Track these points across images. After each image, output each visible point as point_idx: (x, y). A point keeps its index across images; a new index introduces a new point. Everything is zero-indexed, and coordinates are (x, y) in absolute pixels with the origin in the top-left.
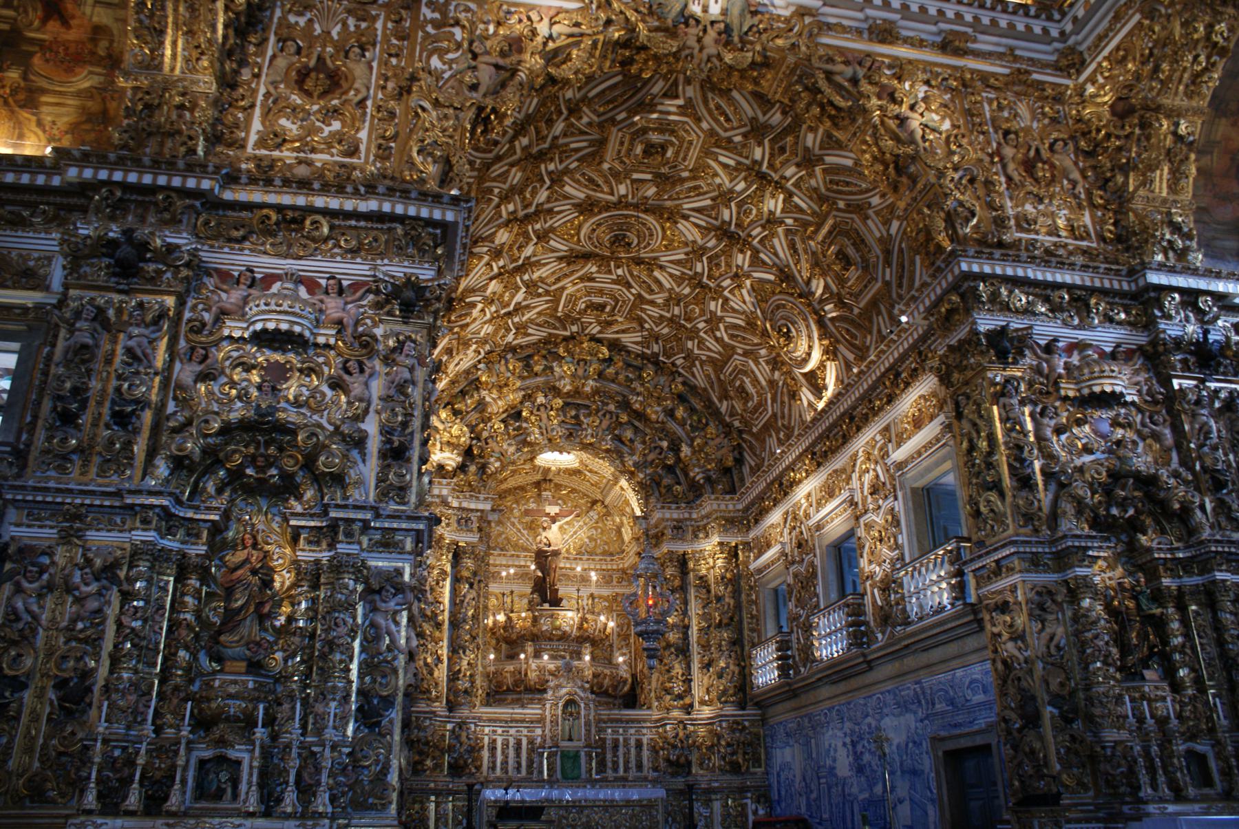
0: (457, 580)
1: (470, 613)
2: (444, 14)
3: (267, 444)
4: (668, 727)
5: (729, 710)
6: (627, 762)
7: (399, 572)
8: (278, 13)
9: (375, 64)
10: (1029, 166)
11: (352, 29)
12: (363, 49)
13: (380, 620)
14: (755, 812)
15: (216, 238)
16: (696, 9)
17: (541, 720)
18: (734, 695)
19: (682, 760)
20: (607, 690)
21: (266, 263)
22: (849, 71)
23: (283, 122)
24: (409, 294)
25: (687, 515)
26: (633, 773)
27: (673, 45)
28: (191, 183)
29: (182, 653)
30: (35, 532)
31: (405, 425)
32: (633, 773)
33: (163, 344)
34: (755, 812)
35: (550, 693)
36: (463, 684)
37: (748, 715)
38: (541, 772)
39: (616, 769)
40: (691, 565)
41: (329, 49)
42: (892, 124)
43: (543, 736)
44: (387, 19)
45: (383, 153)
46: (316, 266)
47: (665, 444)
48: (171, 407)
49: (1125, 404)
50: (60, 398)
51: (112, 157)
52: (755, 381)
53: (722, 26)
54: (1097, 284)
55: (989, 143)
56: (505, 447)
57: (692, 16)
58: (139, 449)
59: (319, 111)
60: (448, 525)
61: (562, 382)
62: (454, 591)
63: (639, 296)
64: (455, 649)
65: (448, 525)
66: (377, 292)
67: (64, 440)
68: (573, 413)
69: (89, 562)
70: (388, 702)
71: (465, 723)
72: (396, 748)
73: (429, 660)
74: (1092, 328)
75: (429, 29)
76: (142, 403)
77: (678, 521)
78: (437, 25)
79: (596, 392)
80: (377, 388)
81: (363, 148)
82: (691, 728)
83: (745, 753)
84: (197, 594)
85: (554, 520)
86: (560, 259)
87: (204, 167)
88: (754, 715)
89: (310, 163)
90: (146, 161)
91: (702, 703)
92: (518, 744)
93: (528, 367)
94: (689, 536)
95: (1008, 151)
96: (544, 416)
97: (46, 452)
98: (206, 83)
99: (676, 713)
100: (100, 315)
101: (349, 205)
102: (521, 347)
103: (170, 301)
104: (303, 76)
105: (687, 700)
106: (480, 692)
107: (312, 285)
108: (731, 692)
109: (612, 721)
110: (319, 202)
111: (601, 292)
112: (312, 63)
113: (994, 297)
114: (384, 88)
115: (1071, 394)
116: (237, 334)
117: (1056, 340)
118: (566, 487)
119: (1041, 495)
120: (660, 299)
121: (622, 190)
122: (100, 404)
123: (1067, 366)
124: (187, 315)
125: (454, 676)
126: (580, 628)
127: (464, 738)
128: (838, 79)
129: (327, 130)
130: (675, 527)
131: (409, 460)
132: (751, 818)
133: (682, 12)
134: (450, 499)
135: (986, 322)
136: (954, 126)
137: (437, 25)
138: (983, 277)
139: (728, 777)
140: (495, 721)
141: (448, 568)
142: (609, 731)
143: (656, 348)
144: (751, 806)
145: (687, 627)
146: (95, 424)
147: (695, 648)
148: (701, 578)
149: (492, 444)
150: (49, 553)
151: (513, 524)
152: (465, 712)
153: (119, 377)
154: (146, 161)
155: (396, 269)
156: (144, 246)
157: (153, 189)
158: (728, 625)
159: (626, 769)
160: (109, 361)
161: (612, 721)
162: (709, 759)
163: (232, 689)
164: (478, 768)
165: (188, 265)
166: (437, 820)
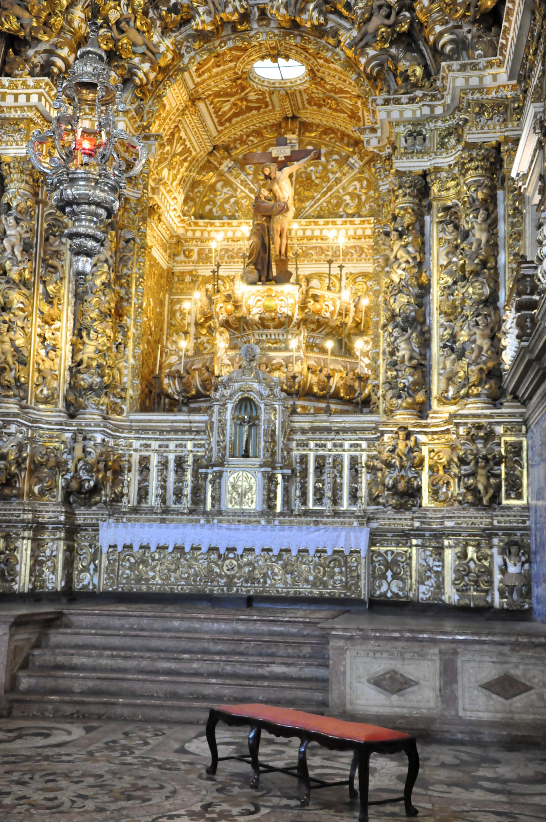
1: (98, 282)
4: (386, 437)
14: (504, 570)
18: (480, 383)
19: (402, 486)
20: (337, 392)
25: (426, 111)
26: (345, 505)
34: (504, 570)
35: (221, 389)
37: (500, 415)
38: (204, 502)
40: (435, 189)
71: (80, 431)
73: (20, 342)
77: (417, 123)
82: (422, 438)
83: (491, 475)
85: (282, 165)
88: (511, 415)
91: (444, 400)
92: (180, 463)
94: (433, 141)
105: (420, 397)
106: (130, 392)
108: (473, 378)
118: (318, 126)
126: (303, 306)
127: (78, 452)
130: (410, 134)
132: (497, 576)
139: (472, 512)
140: (145, 430)
142: (312, 444)
144: (498, 560)
148: (446, 209)
158: (476, 274)
161: (314, 430)
162: (448, 483)
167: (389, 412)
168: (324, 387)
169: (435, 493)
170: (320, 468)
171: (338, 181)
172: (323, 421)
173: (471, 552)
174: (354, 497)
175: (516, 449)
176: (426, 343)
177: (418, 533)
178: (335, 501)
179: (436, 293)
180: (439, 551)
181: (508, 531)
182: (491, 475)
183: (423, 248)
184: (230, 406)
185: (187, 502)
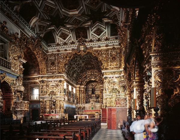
10: (113, 58)
46: (55, 79)
58: (46, 94)
78: (61, 56)
95: (111, 57)
100: (42, 86)
113: (106, 74)
123: (112, 79)
137: (61, 56)
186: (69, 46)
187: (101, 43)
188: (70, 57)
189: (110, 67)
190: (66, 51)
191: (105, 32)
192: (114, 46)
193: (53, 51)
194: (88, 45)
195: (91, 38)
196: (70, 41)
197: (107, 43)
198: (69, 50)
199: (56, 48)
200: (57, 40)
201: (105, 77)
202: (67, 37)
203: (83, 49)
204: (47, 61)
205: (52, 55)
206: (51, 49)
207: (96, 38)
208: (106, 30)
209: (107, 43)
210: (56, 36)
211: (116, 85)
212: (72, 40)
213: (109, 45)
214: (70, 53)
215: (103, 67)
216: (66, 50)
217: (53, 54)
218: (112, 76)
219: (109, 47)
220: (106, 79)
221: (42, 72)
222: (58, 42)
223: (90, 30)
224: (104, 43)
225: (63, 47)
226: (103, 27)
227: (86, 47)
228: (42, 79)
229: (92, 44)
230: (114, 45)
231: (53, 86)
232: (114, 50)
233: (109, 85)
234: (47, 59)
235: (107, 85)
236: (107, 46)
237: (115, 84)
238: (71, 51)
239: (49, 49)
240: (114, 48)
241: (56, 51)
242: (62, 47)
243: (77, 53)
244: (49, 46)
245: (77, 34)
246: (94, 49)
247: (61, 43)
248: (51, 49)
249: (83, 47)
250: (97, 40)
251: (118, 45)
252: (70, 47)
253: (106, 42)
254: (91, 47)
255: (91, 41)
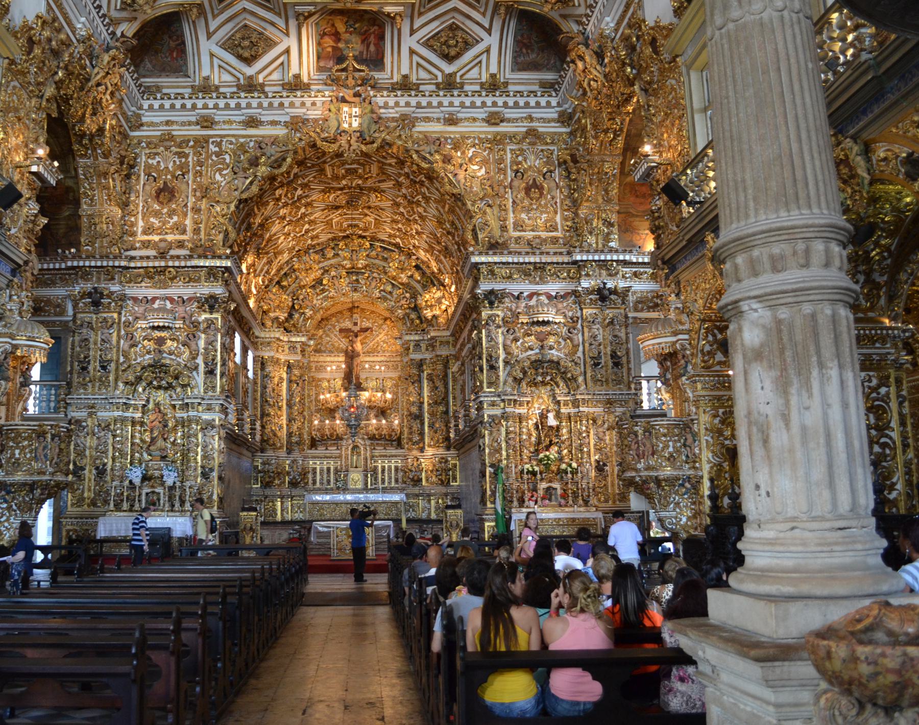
0: (290, 381)
2: (220, 148)
3: (160, 372)
5: (441, 451)
6: (390, 478)
7: (214, 420)
8: (144, 159)
9: (190, 182)
10: (528, 190)
11: (178, 163)
12: (183, 175)
13: (208, 441)
15: (130, 282)
16: (346, 126)
17: (340, 457)
19: (416, 478)
21: (152, 292)
22: (428, 149)
23: (152, 220)
24: (212, 301)
27: (334, 147)
28: (117, 264)
29: (137, 454)
30: (79, 414)
31: (213, 360)
32: (393, 484)
33: (115, 334)
36: (294, 439)
39: (383, 482)
40: (425, 367)
41: (169, 177)
42: (450, 175)
43: (341, 465)
44: (194, 154)
45: (197, 231)
47: (408, 295)
48: (122, 359)
49: (556, 323)
50: (80, 362)
51: (84, 256)
52: (444, 266)
53: (358, 134)
54: (549, 261)
55: (506, 178)
56: (315, 302)
57: (344, 131)
58: (111, 378)
59: (167, 213)
60: (283, 351)
61: (345, 262)
62: (289, 389)
63: (376, 219)
64: (290, 420)
65: (283, 351)
66: (198, 302)
67: (84, 379)
68: (354, 278)
69: (99, 425)
70: (212, 470)
72: (216, 486)
74: (545, 283)
75: (214, 158)
76: (110, 361)
78: (218, 154)
79: (365, 267)
80: (202, 344)
81: (188, 229)
83: (447, 475)
84: (140, 432)
85: (356, 336)
86: (323, 210)
87: (121, 257)
89: (165, 240)
90: (98, 256)
91: (430, 446)
93: (323, 255)
94: (423, 349)
95: (516, 183)
96: (336, 283)
97: (79, 383)
98: (118, 212)
99: (415, 453)
101: (183, 264)
102: (318, 244)
103: (115, 315)
104: (159, 192)
105: (421, 445)
107: (172, 300)
109: (381, 456)
110: (170, 264)
111: (353, 219)
112: (162, 186)
113: (492, 272)
114: (195, 196)
115: (525, 321)
116: (144, 326)
117: (522, 293)
119: (501, 373)
120: (388, 220)
121: (344, 182)
122: (95, 362)
123: (527, 307)
124: (123, 319)
125: (290, 435)
127: (295, 468)
128: (423, 153)
129: (172, 221)
131: (216, 375)
133: (338, 128)
134: (281, 338)
135: (485, 286)
136: (487, 173)
137: (218, 154)
138: (482, 263)
139: (440, 487)
140: (315, 457)
141: (285, 376)
143: (398, 240)
145: (423, 403)
146: (94, 370)
147: (426, 415)
149: (307, 302)
150: (85, 421)
151: (336, 336)
152: (296, 454)
153: (101, 350)
154: (98, 256)
155: (205, 289)
156: (102, 294)
157: (102, 267)
159: (390, 483)
160: (95, 344)
161: (381, 456)
163: (156, 467)
164: (307, 483)
165: (120, 300)
166: (282, 510)
167: (410, 450)
168: (381, 435)
169: (427, 480)
170: (383, 471)
171: (378, 336)
172: (383, 452)
173: (440, 501)
174: (397, 481)
175: (455, 466)
176: (422, 424)
177: (421, 495)
178: (390, 483)
179: (426, 406)
180: (429, 501)
181: (453, 494)
182: (447, 475)
183: (421, 388)
184: (350, 448)
185: (332, 485)
186: (276, 102)
187: (462, 105)
188: (278, 163)
189: (517, 234)
190: (256, 127)
191: (488, 51)
192: (534, 124)
193: (168, 123)
194: (386, 103)
195: (405, 70)
196: (276, 76)
197: (495, 104)
198: (274, 123)
199: (194, 107)
200: (205, 59)
201: (492, 292)
202: (265, 52)
203: (355, 124)
204: (128, 176)
205: (167, 139)
206: (162, 107)
207: (430, 72)
208: (492, 41)
209: (495, 104)
210: (202, 37)
211: (551, 340)
212: (294, 69)
213: (507, 116)
214: (275, 141)
215: (474, 230)
216: (253, 122)
217: (172, 138)
218: (525, 287)
219: (504, 128)
220: (491, 304)
221: (92, 243)
222: (206, 72)
223: (406, 30)
224: (478, 104)
225: (238, 106)
226: (478, 23)
227: (372, 112)
228: (89, 286)
229: (413, 101)
230: (530, 118)
231: (157, 334)
232: (534, 144)
233: (516, 340)
234: (132, 167)
235: (500, 339)
236: (494, 119)
237: (550, 334)
238: (281, 131)
239: (151, 107)
240: (532, 132)
241: (190, 123)
242: (232, 103)
243: (319, 143)
244: (150, 92)
245: (329, 42)
246: (421, 127)
247: (226, 77)
248: (162, 107)
249: (356, 110)
250: (437, 85)
251: (553, 120)
252: (281, 105)
253: (489, 101)
254: (404, 117)
255: (405, 86)
